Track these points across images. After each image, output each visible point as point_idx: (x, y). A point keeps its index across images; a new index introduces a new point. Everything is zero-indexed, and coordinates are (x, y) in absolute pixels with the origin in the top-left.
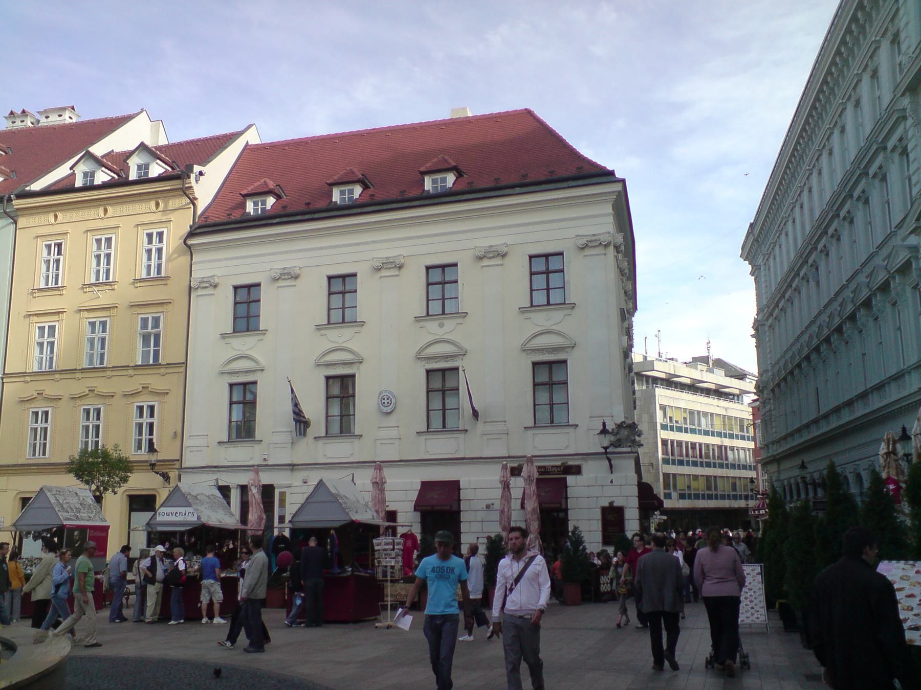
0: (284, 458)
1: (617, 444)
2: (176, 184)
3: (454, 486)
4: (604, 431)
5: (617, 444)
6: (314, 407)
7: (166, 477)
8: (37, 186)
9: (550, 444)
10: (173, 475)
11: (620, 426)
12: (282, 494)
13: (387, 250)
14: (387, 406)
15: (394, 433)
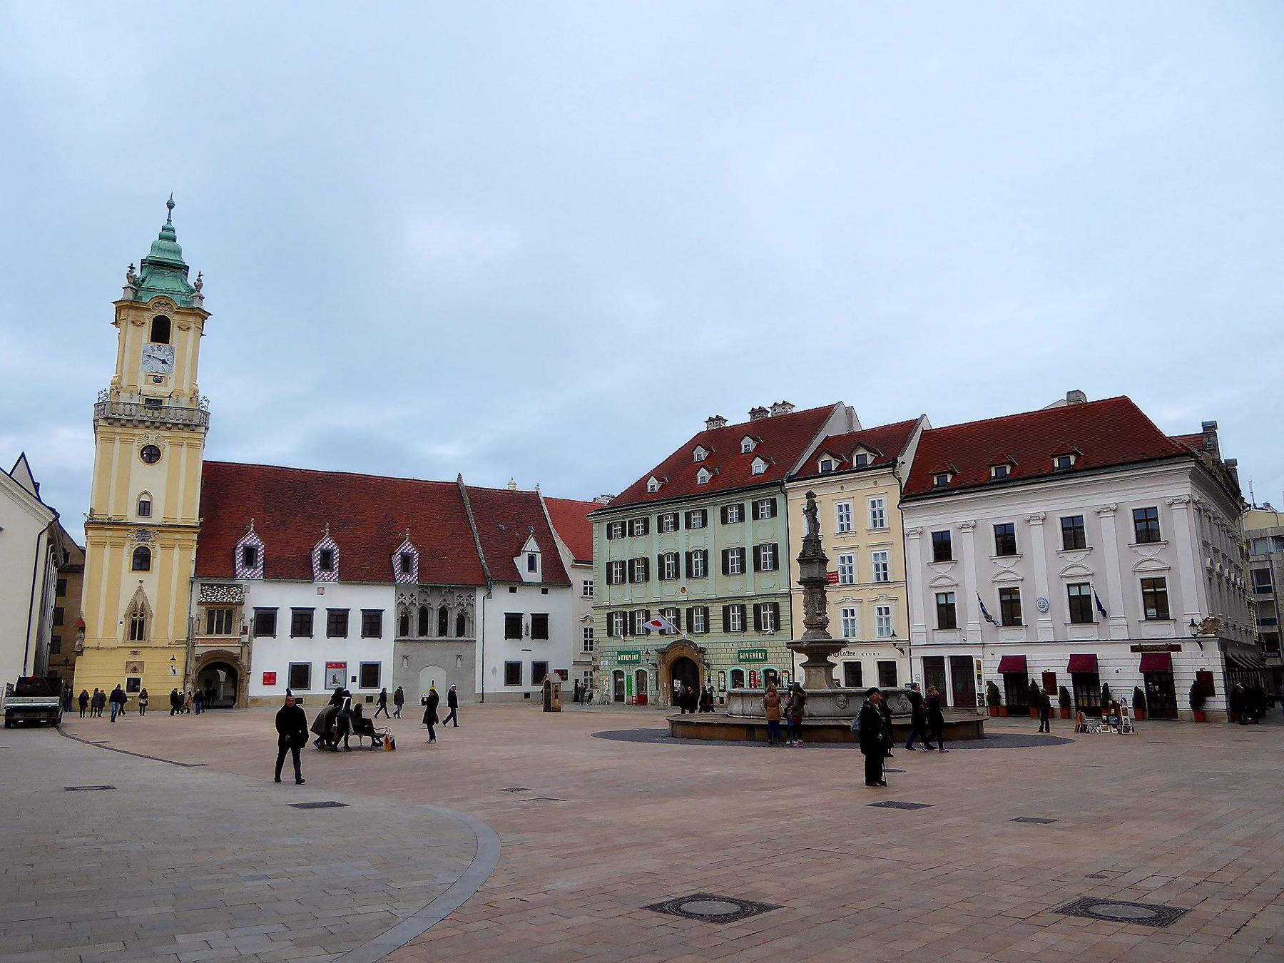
0: (975, 638)
1: (1205, 632)
2: (890, 470)
3: (1093, 659)
4: (1193, 625)
5: (1205, 632)
6: (996, 610)
7: (901, 650)
8: (794, 472)
9: (1157, 632)
10: (906, 649)
11: (1205, 621)
12: (978, 662)
13: (1035, 511)
14: (1045, 608)
15: (1050, 624)
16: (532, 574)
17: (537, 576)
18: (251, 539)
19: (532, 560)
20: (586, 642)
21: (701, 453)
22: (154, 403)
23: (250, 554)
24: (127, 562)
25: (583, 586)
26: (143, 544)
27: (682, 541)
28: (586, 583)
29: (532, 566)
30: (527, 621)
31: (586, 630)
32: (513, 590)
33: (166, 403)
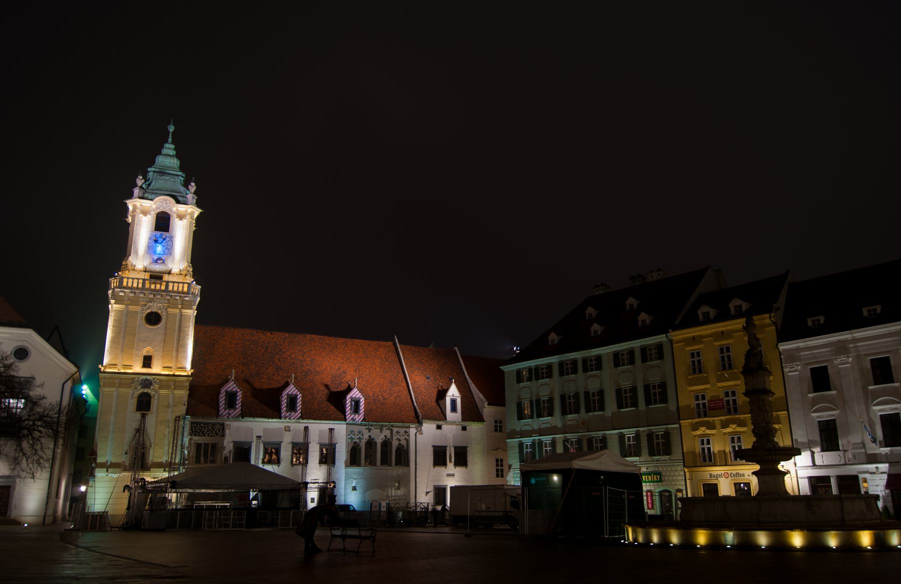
8: (677, 322)
16: (453, 414)
17: (457, 416)
18: (231, 386)
19: (453, 402)
20: (497, 470)
21: (590, 311)
22: (156, 277)
23: (231, 399)
24: (133, 403)
25: (493, 424)
26: (146, 390)
27: (580, 383)
28: (496, 422)
29: (454, 409)
30: (451, 452)
31: (497, 460)
32: (439, 427)
33: (166, 278)
